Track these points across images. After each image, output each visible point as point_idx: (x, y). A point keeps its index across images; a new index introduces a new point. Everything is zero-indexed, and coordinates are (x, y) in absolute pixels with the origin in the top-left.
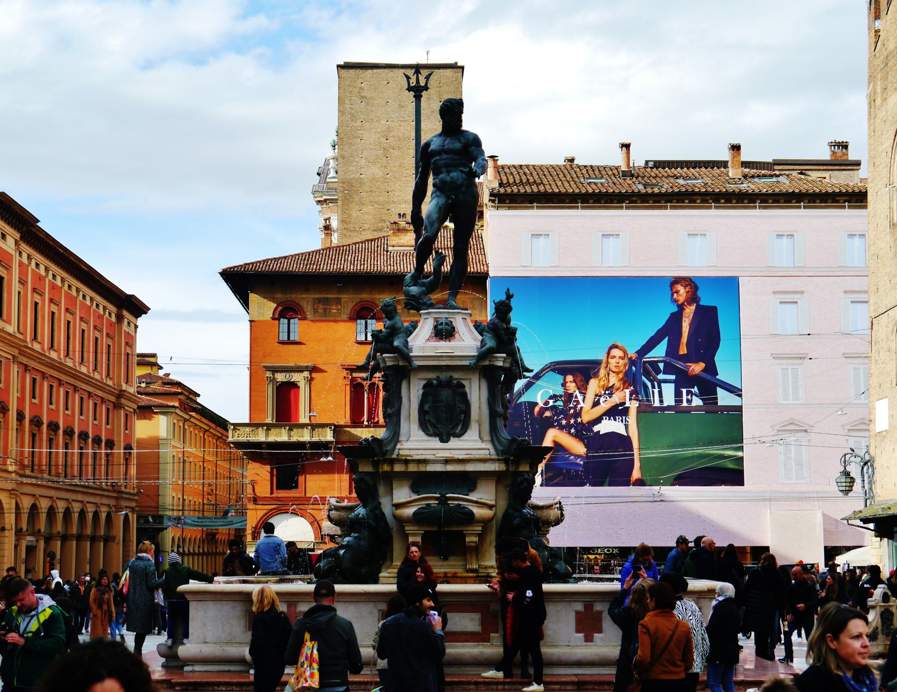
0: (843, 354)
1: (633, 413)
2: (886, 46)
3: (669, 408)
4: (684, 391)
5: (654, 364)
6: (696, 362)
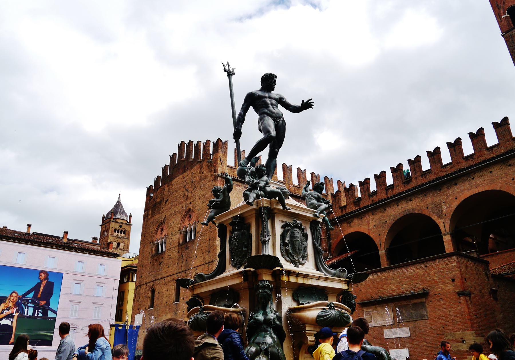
0: (93, 302)
1: (16, 318)
2: (155, 200)
3: (30, 316)
4: (37, 311)
5: (27, 300)
6: (43, 300)
